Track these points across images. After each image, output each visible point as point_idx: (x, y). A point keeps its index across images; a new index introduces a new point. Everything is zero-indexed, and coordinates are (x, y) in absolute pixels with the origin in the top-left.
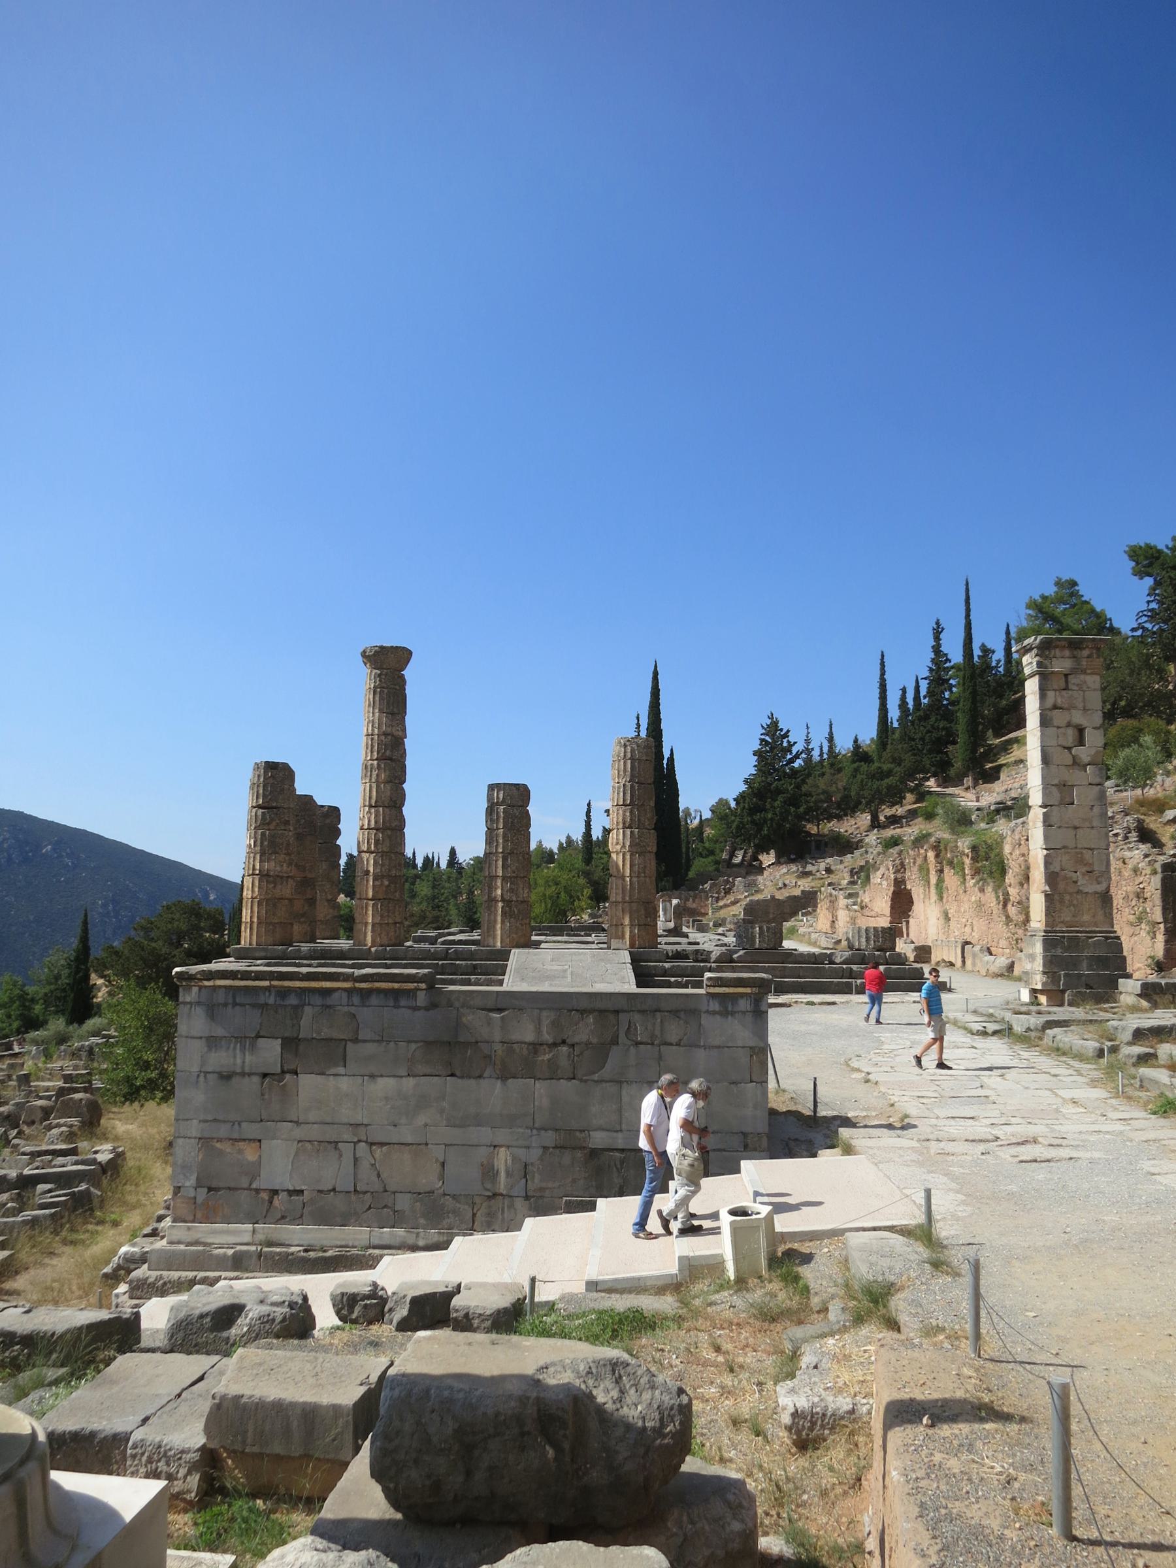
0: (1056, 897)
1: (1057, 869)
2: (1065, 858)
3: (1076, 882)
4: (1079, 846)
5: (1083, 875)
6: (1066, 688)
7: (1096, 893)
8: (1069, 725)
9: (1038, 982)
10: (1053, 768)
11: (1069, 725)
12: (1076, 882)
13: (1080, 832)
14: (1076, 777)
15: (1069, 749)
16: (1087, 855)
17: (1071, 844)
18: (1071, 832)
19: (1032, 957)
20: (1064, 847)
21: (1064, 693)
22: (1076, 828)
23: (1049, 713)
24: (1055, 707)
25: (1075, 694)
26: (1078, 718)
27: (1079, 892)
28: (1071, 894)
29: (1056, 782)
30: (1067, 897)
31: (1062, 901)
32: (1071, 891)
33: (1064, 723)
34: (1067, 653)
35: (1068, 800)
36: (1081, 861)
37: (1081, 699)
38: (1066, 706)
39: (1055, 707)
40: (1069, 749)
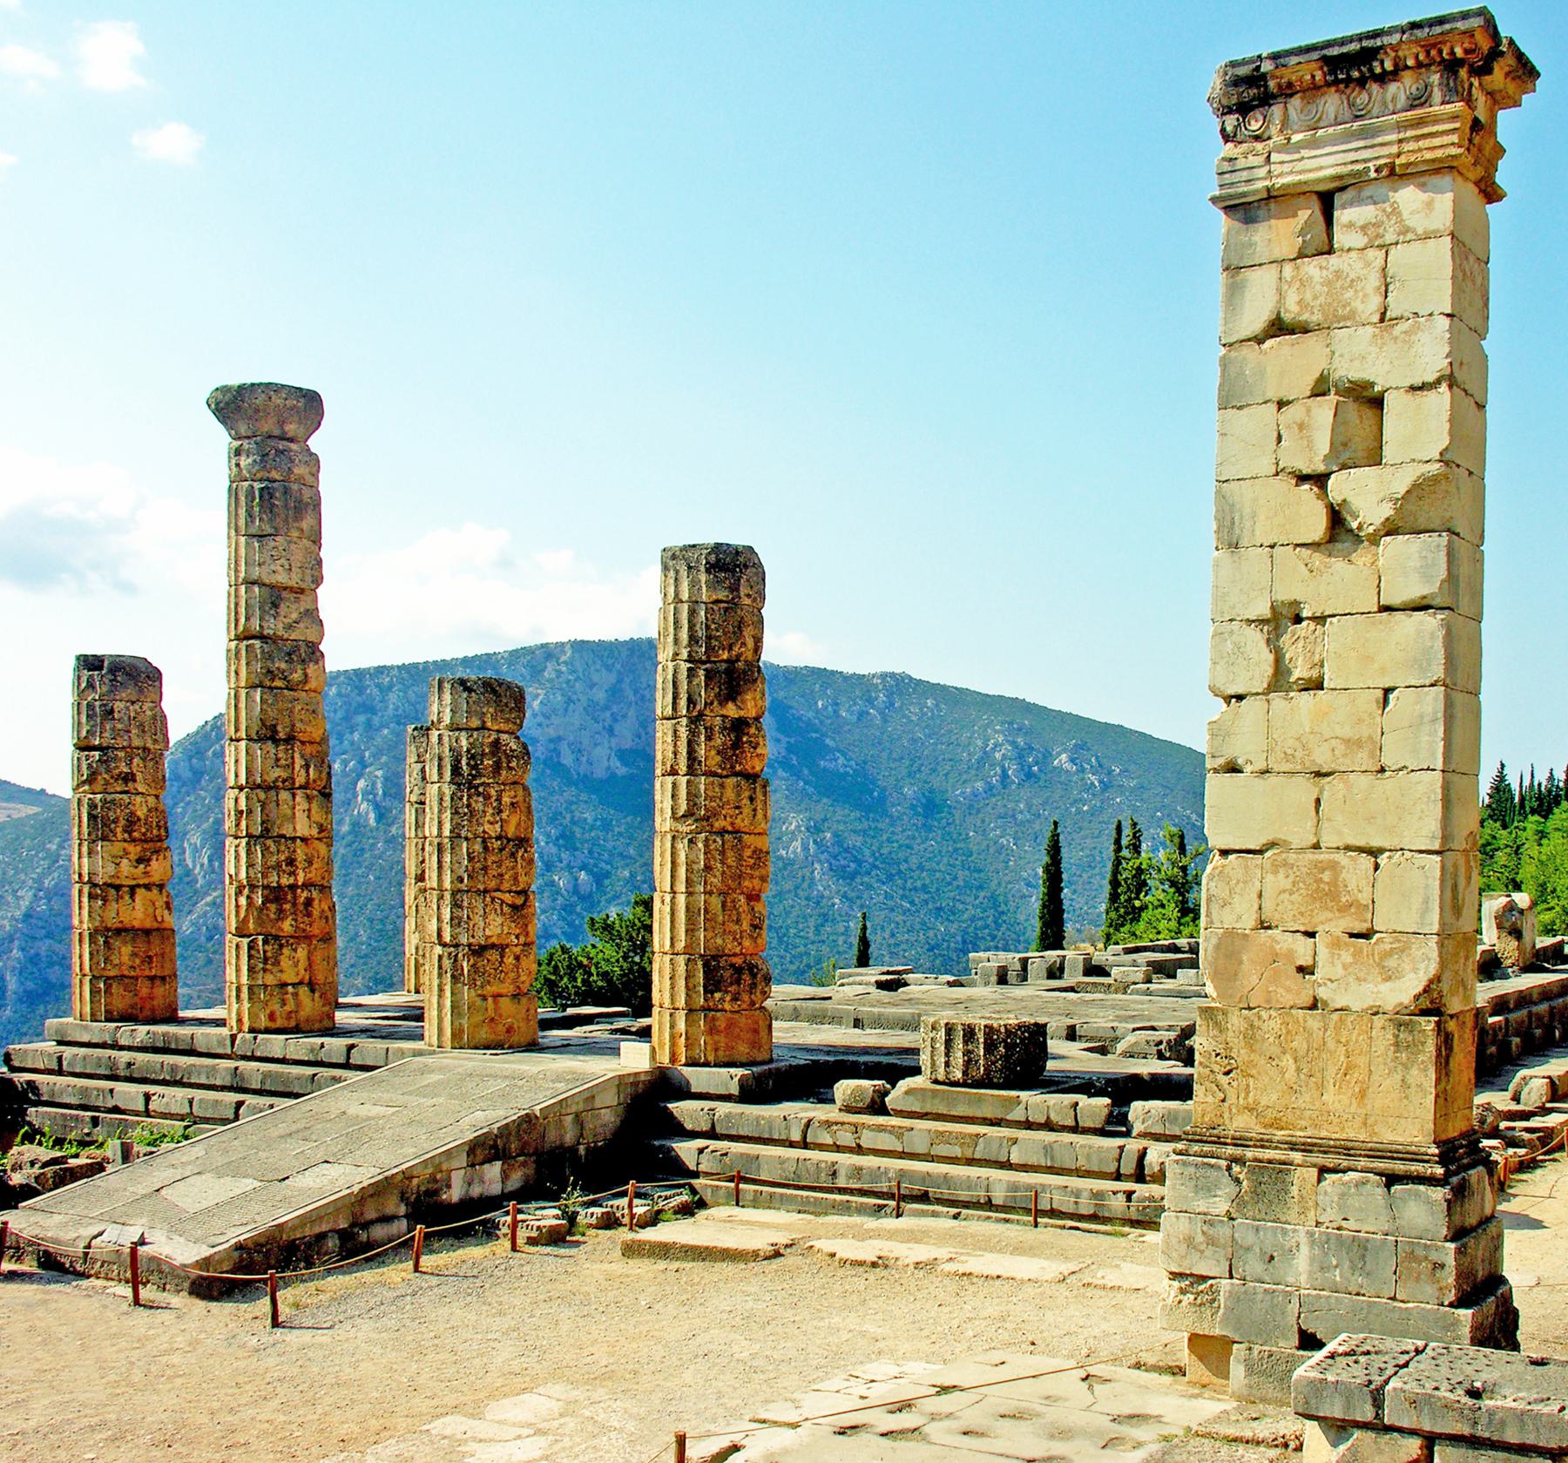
0: (1236, 1021)
2: (1276, 882)
4: (1328, 840)
5: (1335, 944)
6: (1330, 251)
8: (1320, 389)
10: (1255, 559)
11: (1320, 389)
13: (1332, 789)
14: (1339, 582)
17: (1301, 835)
18: (1304, 791)
20: (1273, 845)
21: (1311, 267)
22: (1318, 774)
23: (1250, 353)
26: (1358, 355)
30: (1272, 1024)
31: (1251, 1035)
32: (1288, 999)
34: (1331, 103)
36: (1329, 894)
37: (1374, 281)
38: (1314, 318)
40: (1320, 480)
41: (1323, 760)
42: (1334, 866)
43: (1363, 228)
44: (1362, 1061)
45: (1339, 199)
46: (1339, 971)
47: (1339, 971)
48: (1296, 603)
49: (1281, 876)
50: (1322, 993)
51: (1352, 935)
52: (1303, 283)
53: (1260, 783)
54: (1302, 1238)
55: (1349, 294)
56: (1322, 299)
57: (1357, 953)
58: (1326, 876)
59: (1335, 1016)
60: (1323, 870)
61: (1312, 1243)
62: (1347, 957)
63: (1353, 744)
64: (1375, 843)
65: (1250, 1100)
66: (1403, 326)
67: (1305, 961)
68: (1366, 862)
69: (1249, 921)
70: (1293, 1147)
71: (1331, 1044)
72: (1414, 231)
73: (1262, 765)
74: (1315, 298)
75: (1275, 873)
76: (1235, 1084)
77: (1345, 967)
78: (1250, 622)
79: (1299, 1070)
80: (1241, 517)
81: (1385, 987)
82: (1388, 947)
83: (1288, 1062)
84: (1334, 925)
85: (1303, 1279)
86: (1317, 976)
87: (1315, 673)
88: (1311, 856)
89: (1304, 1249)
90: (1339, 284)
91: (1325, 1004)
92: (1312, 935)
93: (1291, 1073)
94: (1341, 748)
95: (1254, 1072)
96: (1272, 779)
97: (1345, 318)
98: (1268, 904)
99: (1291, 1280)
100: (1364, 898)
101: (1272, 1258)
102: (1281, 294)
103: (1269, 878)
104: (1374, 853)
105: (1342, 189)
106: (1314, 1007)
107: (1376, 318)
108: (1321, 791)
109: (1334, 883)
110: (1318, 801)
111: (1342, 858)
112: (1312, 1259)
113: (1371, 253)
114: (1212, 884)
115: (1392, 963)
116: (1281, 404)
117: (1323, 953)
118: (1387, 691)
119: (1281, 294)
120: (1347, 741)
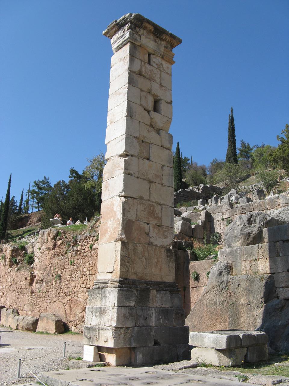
1: (133, 218)
2: (141, 208)
3: (148, 234)
5: (154, 227)
7: (163, 246)
9: (108, 339)
11: (149, 92)
13: (153, 186)
15: (149, 112)
16: (158, 208)
17: (146, 197)
18: (146, 185)
19: (101, 312)
22: (150, 182)
24: (140, 74)
25: (154, 69)
30: (140, 248)
31: (135, 250)
35: (145, 154)
36: (152, 213)
37: (159, 76)
39: (140, 74)
41: (150, 177)
42: (153, 206)
43: (157, 64)
44: (160, 260)
45: (152, 56)
46: (155, 235)
47: (155, 235)
48: (144, 137)
49: (142, 206)
50: (152, 240)
51: (157, 226)
52: (146, 68)
54: (153, 311)
55: (154, 75)
56: (149, 73)
57: (159, 230)
58: (152, 208)
59: (154, 247)
60: (151, 207)
61: (156, 312)
62: (156, 231)
63: (157, 176)
64: (162, 202)
65: (135, 271)
66: (163, 88)
67: (147, 231)
68: (159, 207)
70: (147, 284)
71: (153, 255)
72: (165, 71)
73: (137, 175)
74: (148, 72)
75: (140, 205)
76: (131, 266)
77: (156, 234)
78: (134, 137)
79: (146, 262)
80: (133, 112)
81: (164, 240)
82: (165, 229)
83: (144, 259)
84: (153, 222)
85: (154, 323)
86: (151, 235)
88: (148, 202)
89: (154, 314)
90: (152, 72)
91: (152, 243)
92: (148, 224)
95: (135, 262)
96: (140, 179)
97: (153, 80)
98: (139, 213)
99: (151, 324)
100: (160, 215)
101: (146, 318)
102: (141, 68)
103: (139, 206)
104: (161, 205)
105: (153, 55)
107: (159, 83)
108: (150, 186)
109: (153, 211)
110: (149, 188)
111: (154, 204)
112: (156, 317)
113: (158, 70)
114: (125, 205)
115: (166, 234)
116: (142, 91)
119: (141, 68)
120: (156, 175)
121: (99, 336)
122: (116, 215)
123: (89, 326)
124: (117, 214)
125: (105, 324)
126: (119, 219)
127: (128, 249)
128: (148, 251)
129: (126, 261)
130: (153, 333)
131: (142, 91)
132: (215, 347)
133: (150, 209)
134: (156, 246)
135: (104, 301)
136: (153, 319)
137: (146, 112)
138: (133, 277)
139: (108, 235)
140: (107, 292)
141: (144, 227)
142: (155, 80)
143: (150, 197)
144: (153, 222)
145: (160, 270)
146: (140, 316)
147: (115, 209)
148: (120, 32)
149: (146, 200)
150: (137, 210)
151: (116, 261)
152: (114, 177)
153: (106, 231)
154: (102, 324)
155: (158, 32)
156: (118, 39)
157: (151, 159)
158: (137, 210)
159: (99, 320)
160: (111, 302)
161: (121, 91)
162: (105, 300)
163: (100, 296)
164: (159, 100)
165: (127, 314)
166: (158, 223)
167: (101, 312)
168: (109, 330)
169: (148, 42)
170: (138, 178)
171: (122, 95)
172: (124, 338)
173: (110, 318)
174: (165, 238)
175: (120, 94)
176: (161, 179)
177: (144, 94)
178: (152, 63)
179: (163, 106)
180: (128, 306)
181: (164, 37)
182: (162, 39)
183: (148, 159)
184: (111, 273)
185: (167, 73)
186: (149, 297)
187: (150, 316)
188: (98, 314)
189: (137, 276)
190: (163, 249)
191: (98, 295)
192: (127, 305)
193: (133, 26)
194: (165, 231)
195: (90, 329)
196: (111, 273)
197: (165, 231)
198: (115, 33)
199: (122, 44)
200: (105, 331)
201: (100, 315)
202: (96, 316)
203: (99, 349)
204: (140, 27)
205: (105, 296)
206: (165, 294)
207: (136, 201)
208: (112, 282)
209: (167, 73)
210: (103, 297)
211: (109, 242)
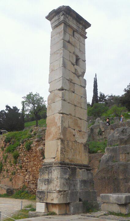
1: (67, 126)
3: (74, 135)
4: (76, 116)
9: (55, 198)
12: (74, 135)
15: (74, 65)
17: (73, 115)
19: (49, 182)
20: (70, 114)
22: (75, 106)
27: (76, 141)
28: (72, 142)
29: (68, 78)
30: (70, 144)
33: (72, 52)
35: (72, 90)
36: (76, 124)
38: (73, 44)
39: (69, 42)
41: (75, 103)
42: (77, 120)
45: (75, 33)
46: (78, 137)
47: (78, 137)
50: (76, 140)
53: (68, 104)
61: (80, 182)
63: (79, 103)
64: (81, 118)
67: (74, 134)
69: (67, 126)
78: (67, 79)
79: (74, 152)
83: (72, 150)
84: (77, 129)
85: (79, 189)
86: (76, 136)
87: (73, 91)
88: (74, 117)
89: (79, 183)
92: (74, 130)
93: (73, 153)
94: (77, 103)
106: (75, 142)
111: (78, 119)
112: (80, 184)
116: (70, 52)
117: (76, 134)
118: (82, 97)
120: (78, 102)
121: (47, 197)
122: (57, 124)
123: (40, 191)
124: (58, 123)
125: (51, 189)
126: (59, 126)
127: (64, 144)
128: (75, 146)
129: (63, 151)
130: (78, 194)
131: (70, 52)
132: (117, 203)
133: (75, 122)
134: (79, 143)
135: (50, 175)
136: (79, 186)
137: (72, 65)
138: (67, 161)
139: (51, 136)
140: (53, 170)
141: (72, 132)
142: (77, 47)
143: (75, 114)
144: (77, 129)
145: (81, 157)
146: (72, 184)
147: (56, 121)
148: (57, 16)
149: (73, 116)
150: (69, 122)
151: (57, 151)
152: (55, 102)
153: (50, 134)
154: (49, 189)
155: (79, 19)
156: (56, 21)
157: (75, 92)
158: (69, 122)
159: (47, 187)
160: (55, 175)
161: (58, 52)
162: (51, 175)
163: (48, 172)
164: (79, 59)
165: (65, 183)
166: (80, 130)
167: (49, 182)
168: (54, 193)
169: (73, 23)
170: (69, 103)
171: (59, 55)
172: (63, 197)
173: (55, 185)
174: (83, 139)
175: (57, 54)
176: (81, 105)
177: (71, 54)
178: (75, 37)
179: (81, 62)
180: (65, 178)
181: (82, 22)
182: (80, 23)
183: (74, 92)
184: (54, 158)
185: (83, 44)
186: (76, 173)
187: (77, 184)
188: (46, 183)
189: (69, 160)
190: (82, 145)
191: (46, 172)
192: (65, 177)
193: (65, 13)
194: (83, 135)
195: (42, 192)
196: (54, 158)
197: (83, 135)
198: (53, 17)
199: (58, 24)
200: (52, 194)
201: (48, 184)
202: (45, 184)
203: (47, 205)
204: (69, 14)
205: (51, 172)
206: (84, 171)
207: (68, 116)
208: (55, 164)
209: (83, 44)
210: (50, 173)
211: (52, 140)
